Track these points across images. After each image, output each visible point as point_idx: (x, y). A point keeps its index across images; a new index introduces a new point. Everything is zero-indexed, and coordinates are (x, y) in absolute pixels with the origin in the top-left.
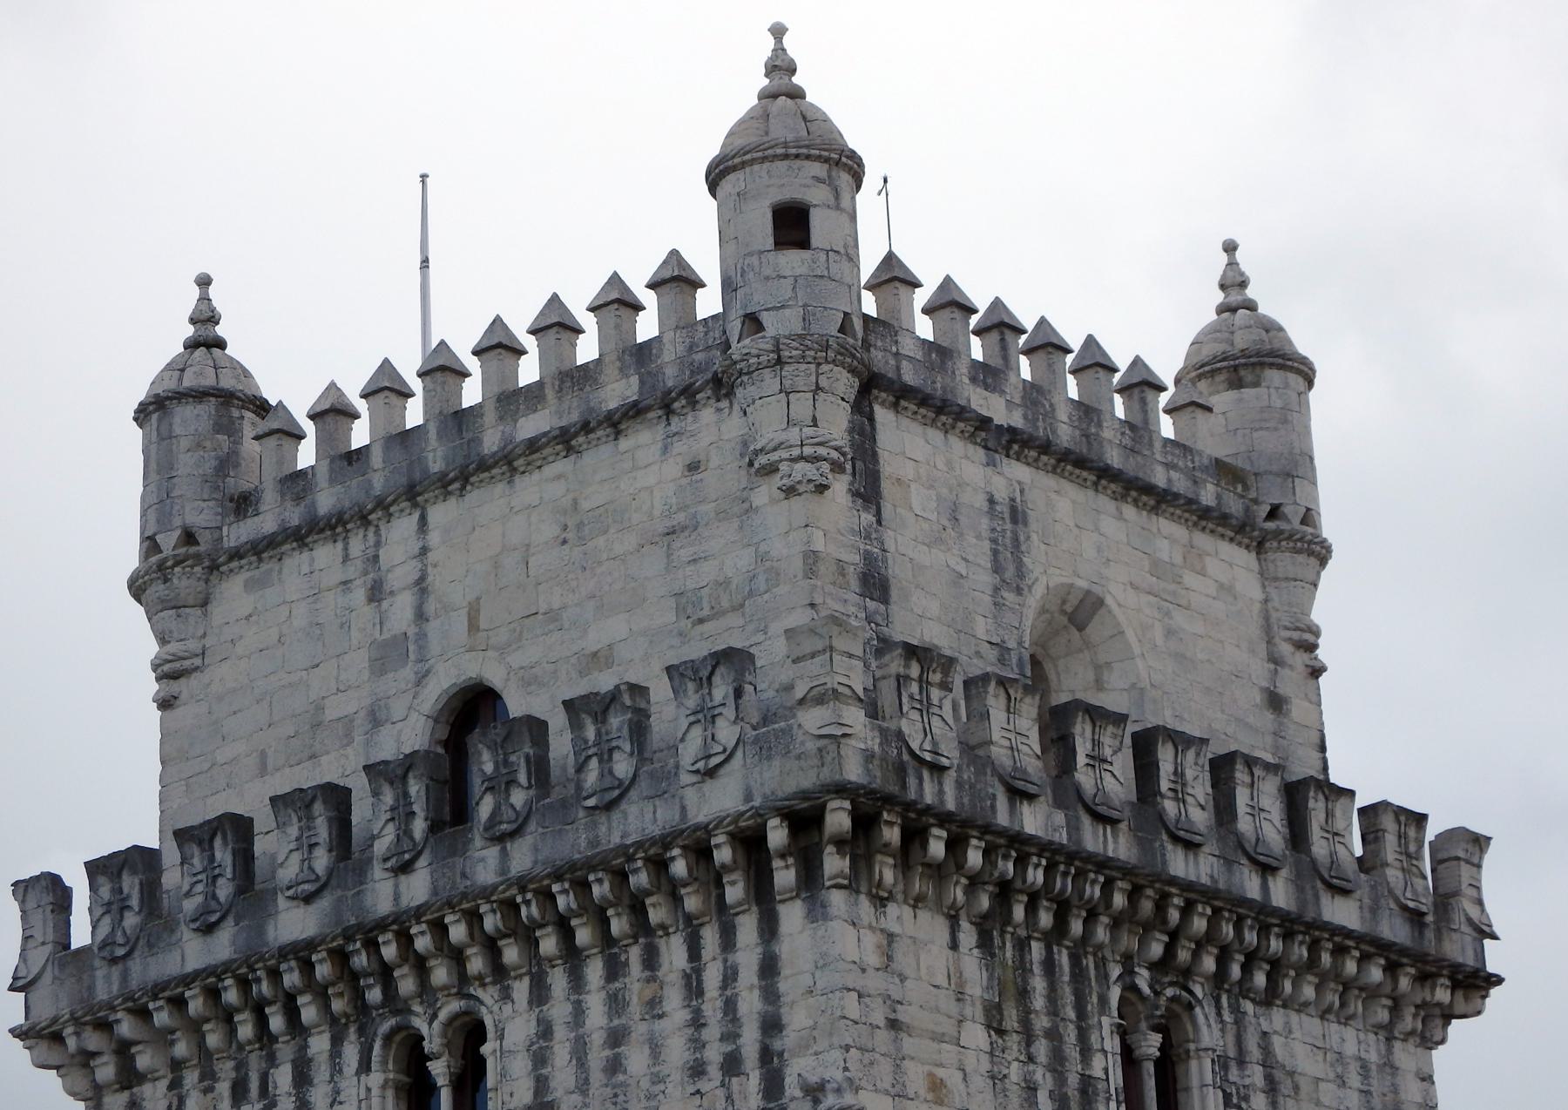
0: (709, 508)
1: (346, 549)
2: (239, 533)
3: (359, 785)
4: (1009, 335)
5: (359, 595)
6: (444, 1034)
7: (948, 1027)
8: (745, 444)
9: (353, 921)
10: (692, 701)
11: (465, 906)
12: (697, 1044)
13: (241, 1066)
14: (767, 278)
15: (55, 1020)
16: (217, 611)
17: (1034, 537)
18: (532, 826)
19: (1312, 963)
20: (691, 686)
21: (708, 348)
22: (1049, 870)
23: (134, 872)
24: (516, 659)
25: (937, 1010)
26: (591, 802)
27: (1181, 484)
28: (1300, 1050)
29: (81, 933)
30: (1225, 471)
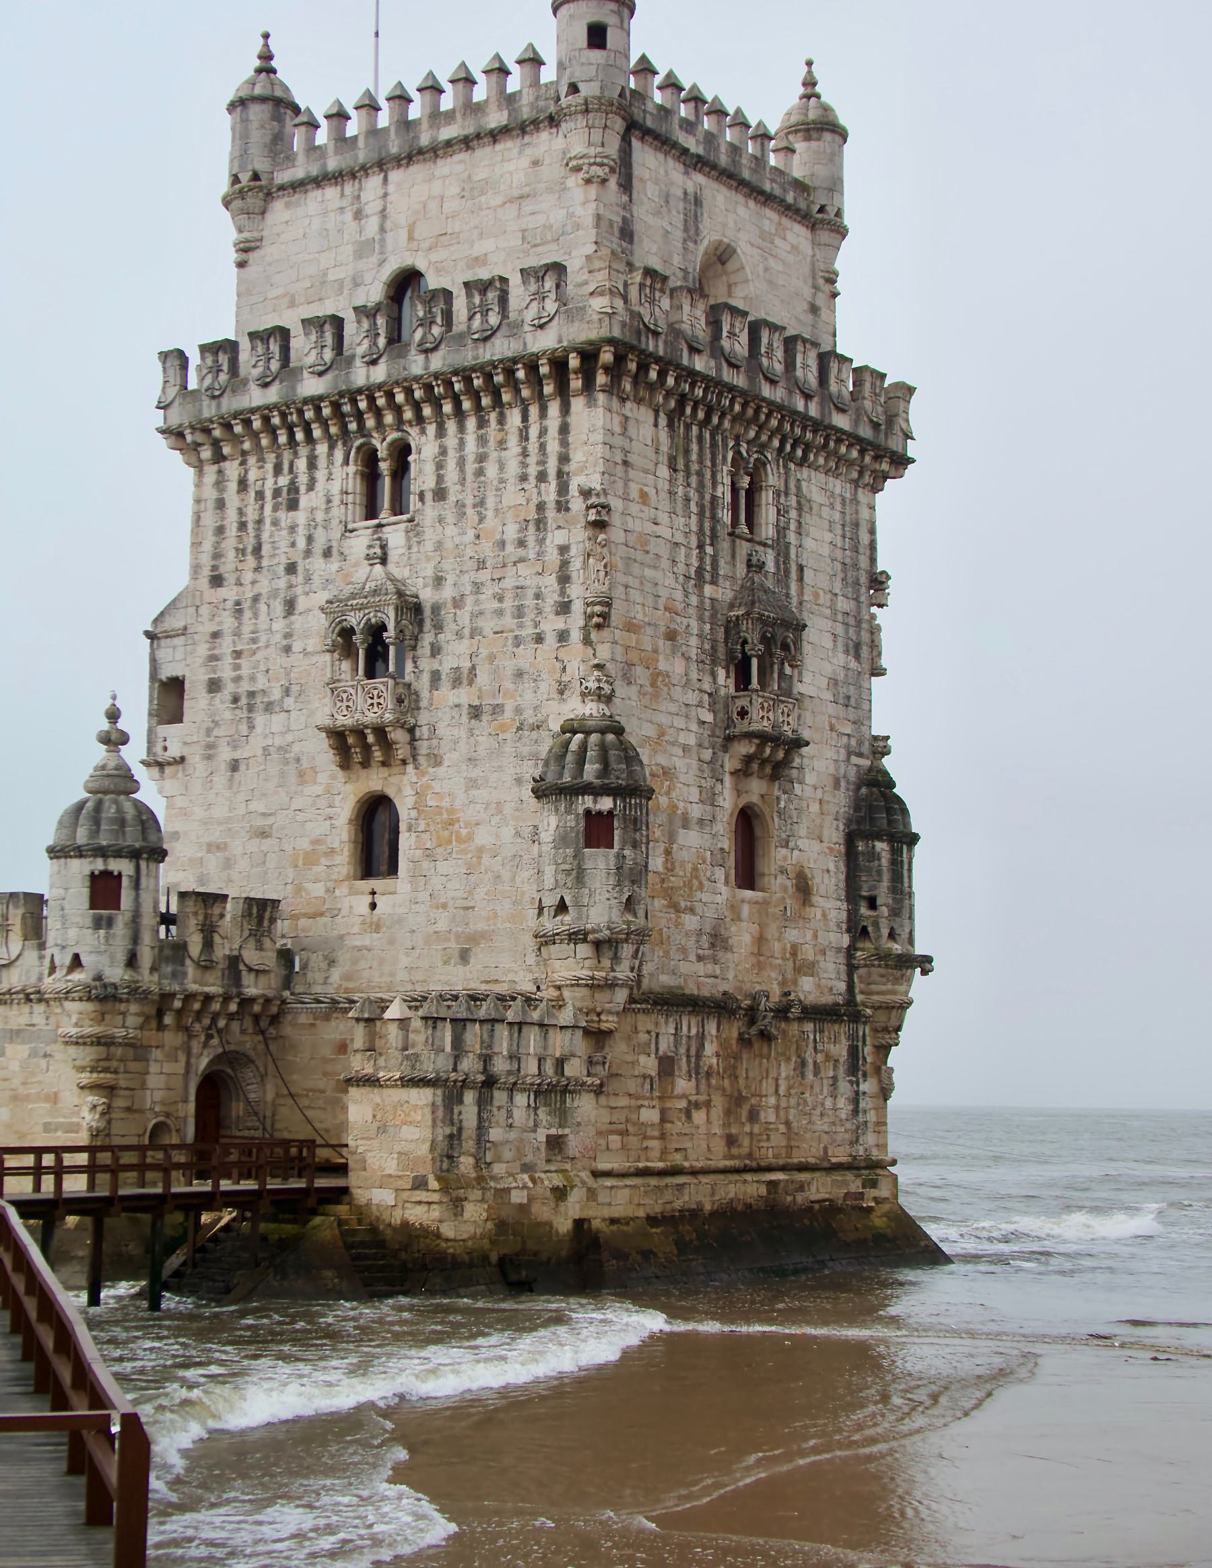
0: (543, 185)
1: (342, 190)
2: (283, 177)
3: (349, 316)
4: (700, 105)
5: (349, 216)
6: (388, 449)
7: (651, 466)
8: (564, 153)
9: (344, 387)
10: (533, 287)
11: (405, 384)
12: (524, 465)
13: (279, 457)
14: (583, 64)
15: (180, 426)
16: (268, 216)
17: (705, 215)
18: (443, 346)
19: (826, 445)
20: (532, 280)
21: (547, 99)
22: (706, 390)
23: (225, 352)
24: (434, 257)
25: (645, 457)
26: (476, 336)
27: (777, 191)
28: (814, 488)
29: (193, 384)
30: (800, 186)
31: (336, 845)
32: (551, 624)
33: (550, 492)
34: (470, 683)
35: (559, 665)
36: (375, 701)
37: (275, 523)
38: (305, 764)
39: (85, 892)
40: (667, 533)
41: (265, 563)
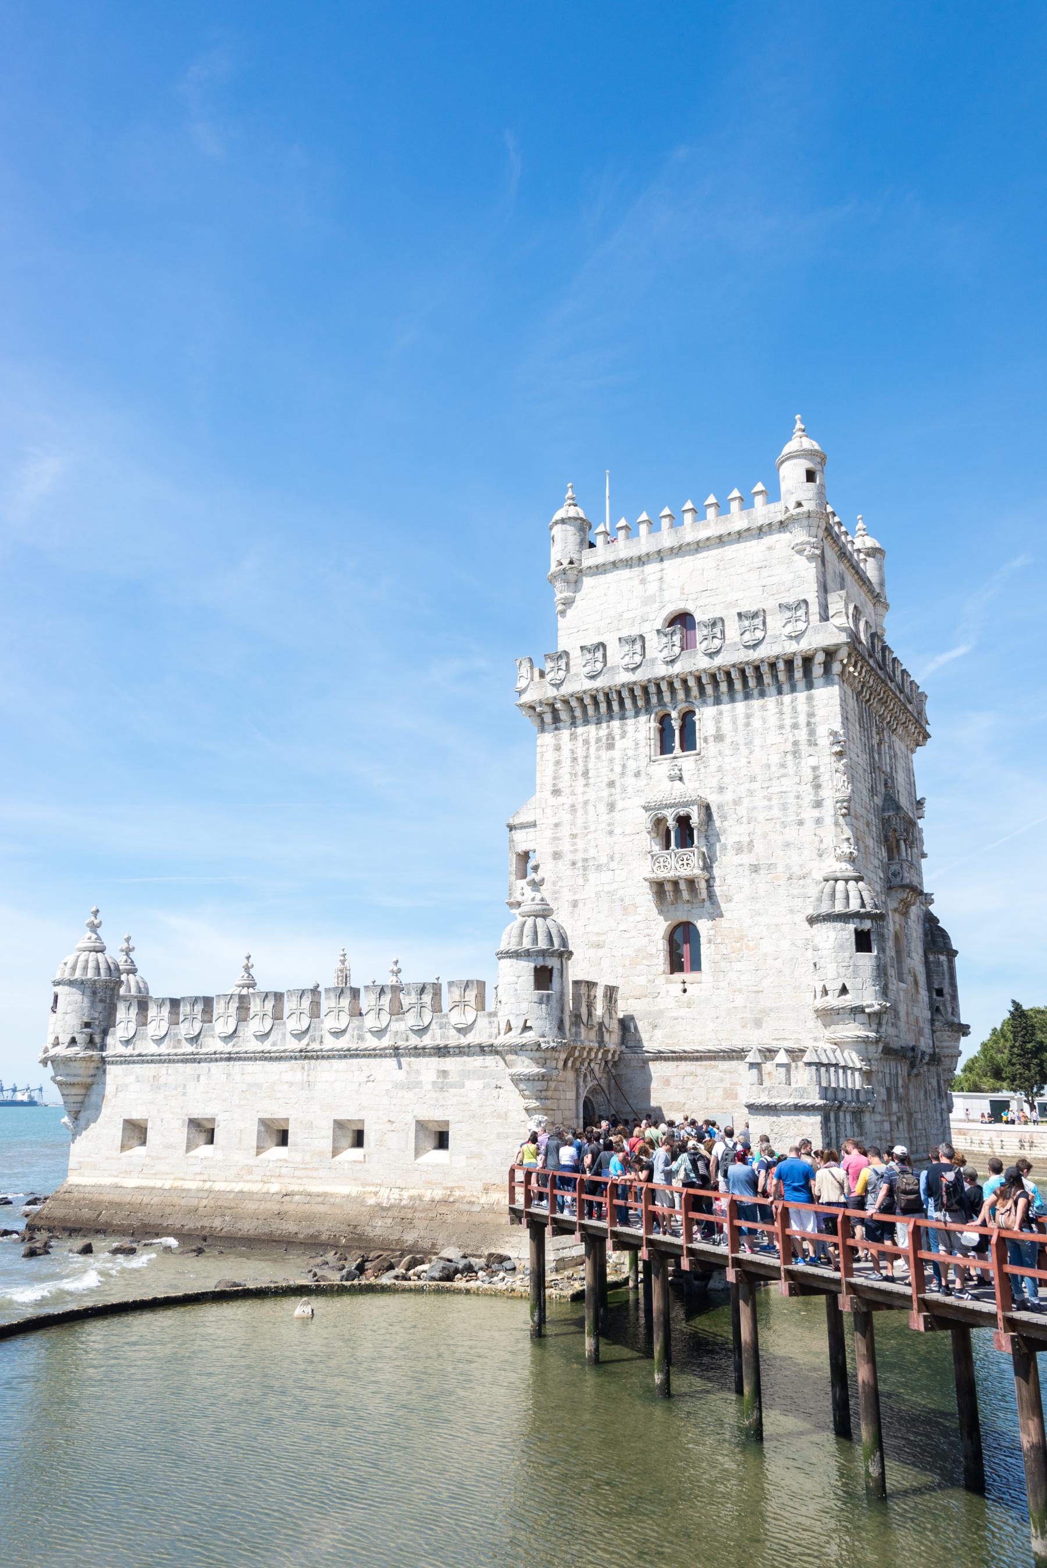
5: (636, 582)
24: (699, 603)
31: (654, 951)
32: (809, 814)
33: (802, 734)
34: (750, 851)
35: (817, 839)
36: (685, 862)
37: (598, 758)
38: (627, 902)
39: (532, 978)
40: (861, 762)
41: (591, 781)
